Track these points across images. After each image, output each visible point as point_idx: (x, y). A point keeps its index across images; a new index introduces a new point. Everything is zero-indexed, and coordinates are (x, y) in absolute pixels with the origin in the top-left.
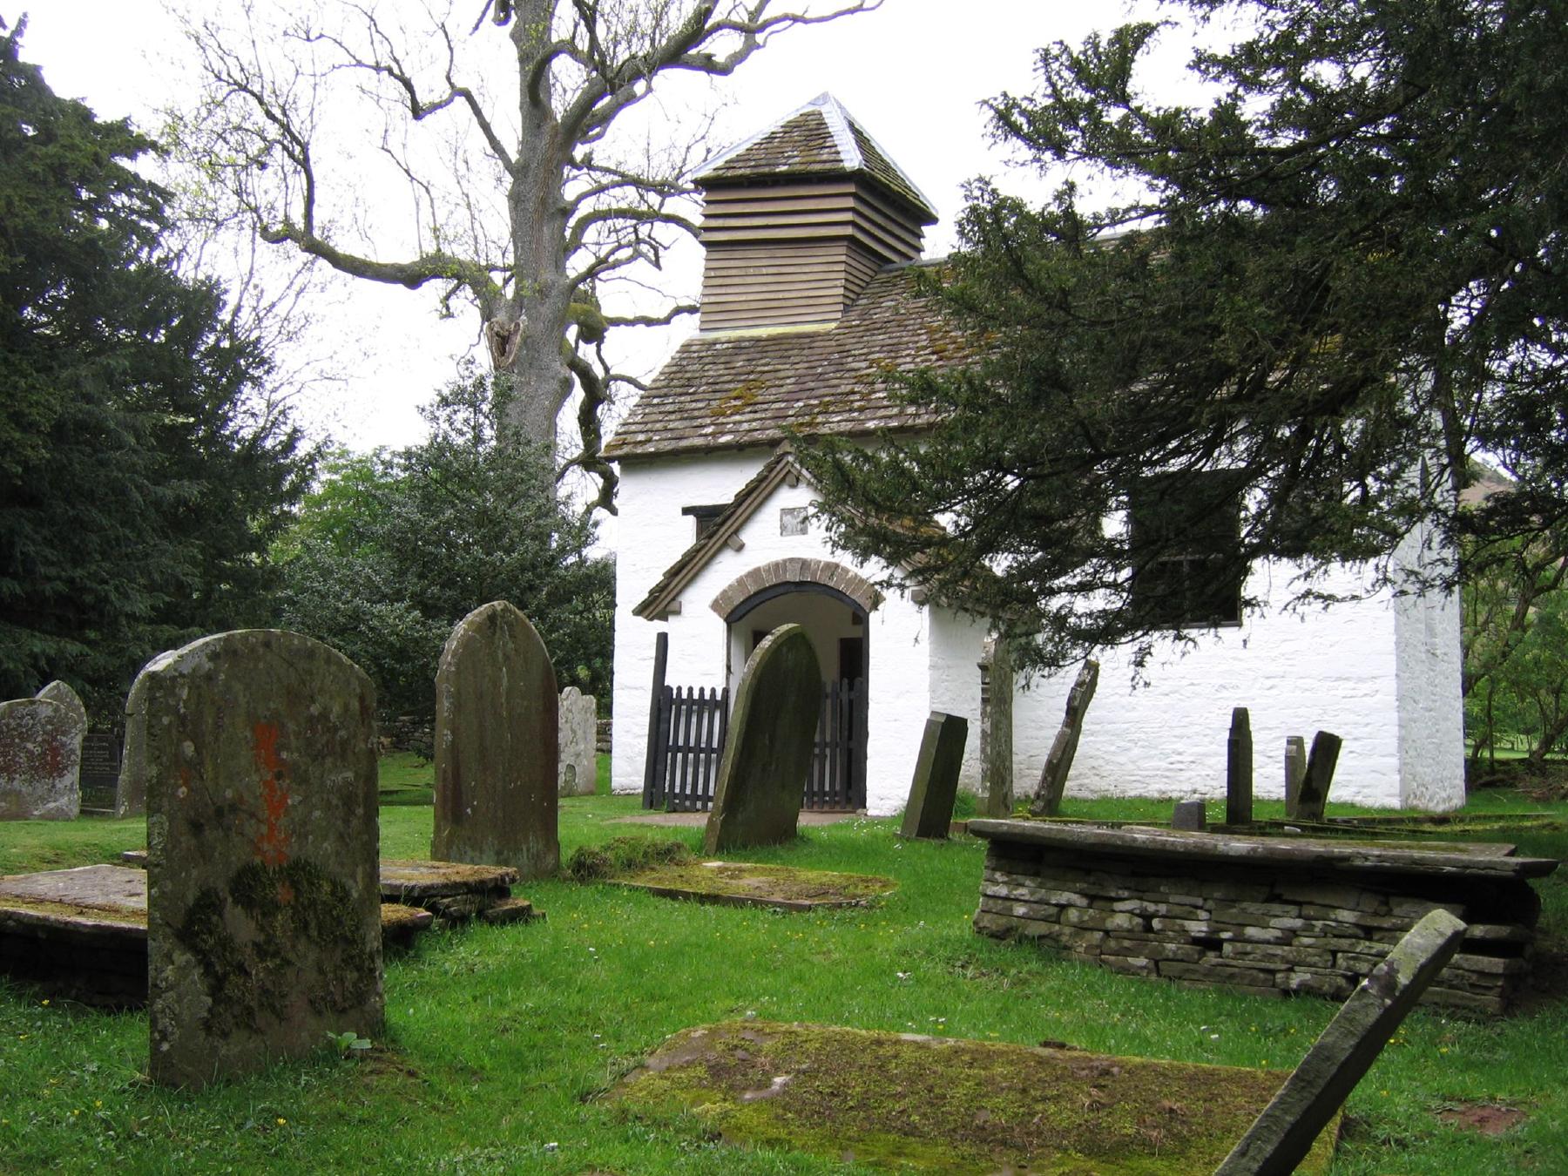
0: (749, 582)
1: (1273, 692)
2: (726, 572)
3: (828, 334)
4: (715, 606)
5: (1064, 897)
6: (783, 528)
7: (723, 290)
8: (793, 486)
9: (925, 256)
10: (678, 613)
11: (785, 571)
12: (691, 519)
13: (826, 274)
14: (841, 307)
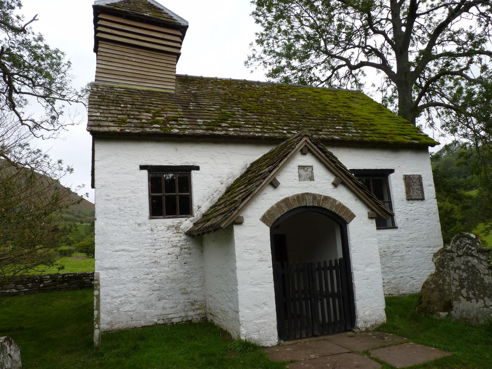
1: (410, 253)
2: (268, 200)
4: (264, 219)
6: (300, 176)
7: (110, 64)
12: (145, 172)
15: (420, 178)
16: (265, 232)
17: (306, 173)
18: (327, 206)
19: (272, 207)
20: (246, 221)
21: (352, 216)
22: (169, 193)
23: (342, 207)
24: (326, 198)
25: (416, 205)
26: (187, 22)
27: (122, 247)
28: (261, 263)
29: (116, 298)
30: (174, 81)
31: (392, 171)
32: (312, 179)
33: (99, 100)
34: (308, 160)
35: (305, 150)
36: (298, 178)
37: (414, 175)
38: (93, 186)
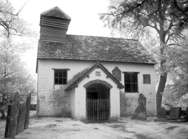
0: (90, 83)
2: (86, 81)
4: (84, 86)
6: (96, 75)
11: (96, 81)
15: (149, 75)
17: (98, 74)
20: (79, 87)
21: (112, 87)
22: (60, 77)
23: (108, 84)
24: (104, 81)
25: (147, 85)
26: (71, 18)
31: (139, 73)
32: (100, 75)
33: (41, 47)
34: (99, 70)
37: (147, 75)
38: (37, 72)
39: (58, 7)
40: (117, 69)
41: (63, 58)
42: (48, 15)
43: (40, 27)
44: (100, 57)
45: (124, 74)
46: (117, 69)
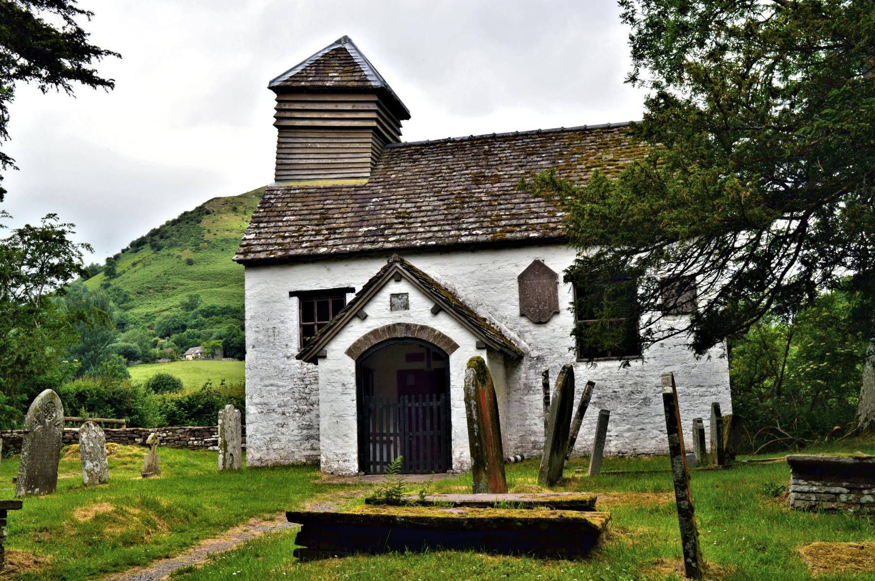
3: (364, 186)
4: (350, 352)
5: (837, 489)
6: (392, 305)
8: (398, 281)
9: (404, 139)
10: (324, 357)
12: (295, 300)
13: (361, 151)
14: (369, 170)
16: (350, 365)
18: (424, 336)
19: (359, 340)
21: (455, 347)
24: (423, 328)
27: (272, 382)
28: (344, 396)
29: (265, 434)
30: (369, 165)
32: (406, 307)
35: (397, 276)
36: (389, 308)
39: (350, 37)
40: (538, 267)
41: (323, 250)
42: (295, 84)
43: (276, 131)
44: (466, 229)
45: (574, 285)
46: (538, 267)
